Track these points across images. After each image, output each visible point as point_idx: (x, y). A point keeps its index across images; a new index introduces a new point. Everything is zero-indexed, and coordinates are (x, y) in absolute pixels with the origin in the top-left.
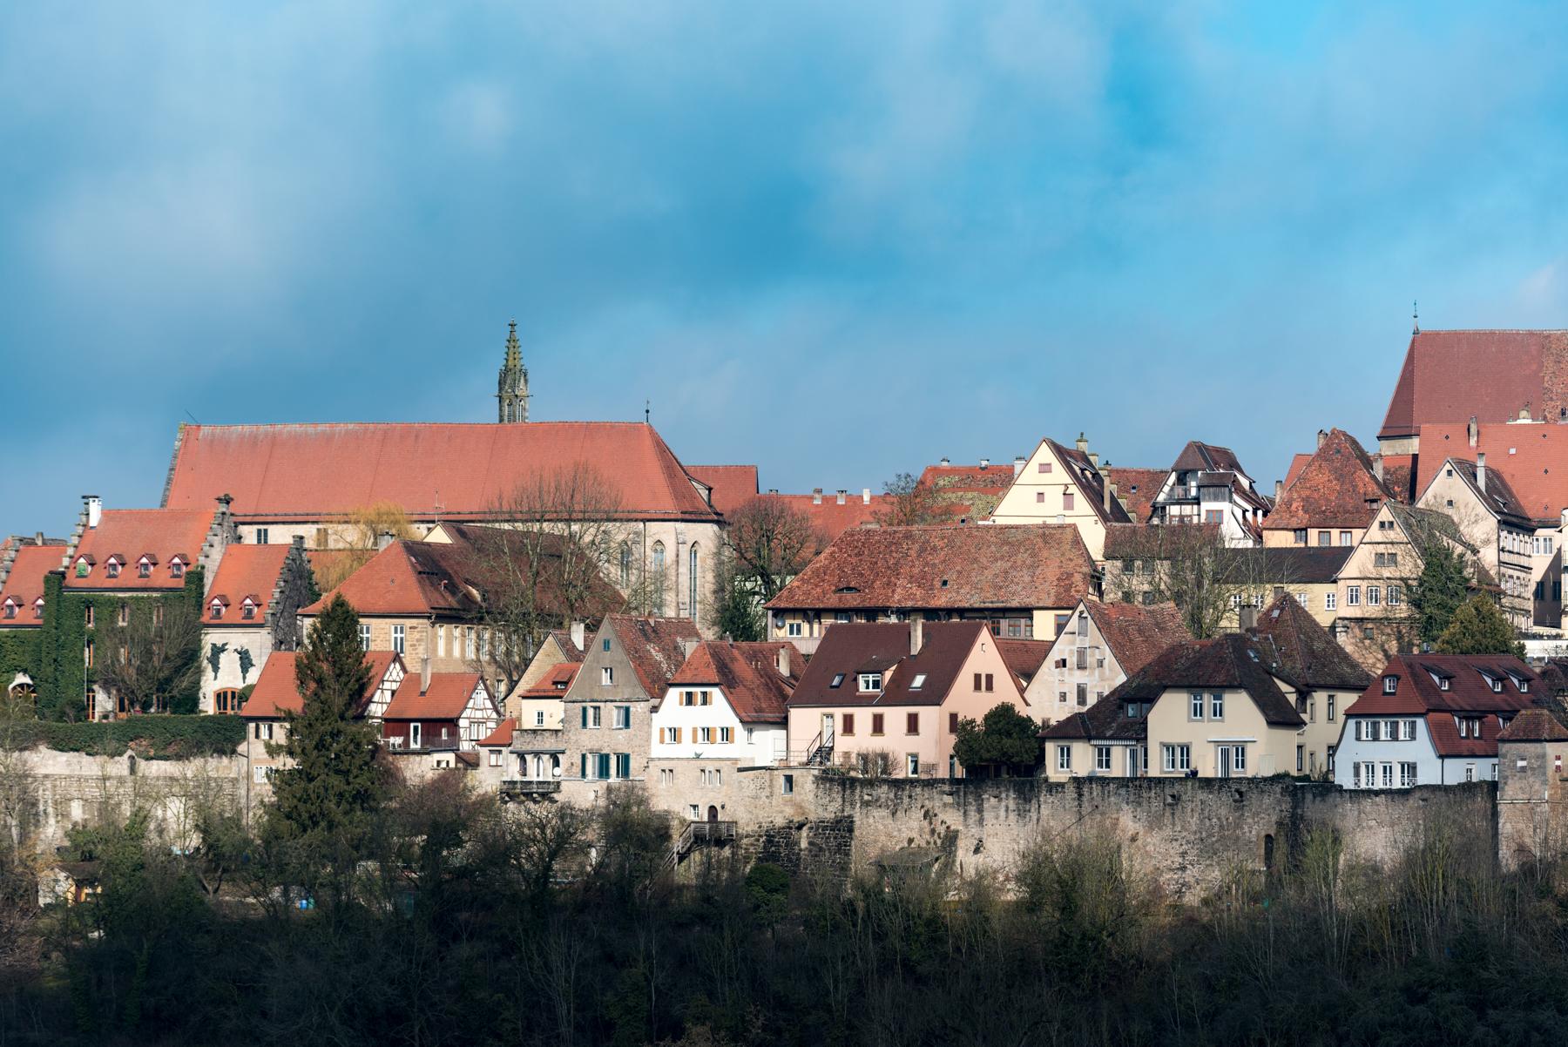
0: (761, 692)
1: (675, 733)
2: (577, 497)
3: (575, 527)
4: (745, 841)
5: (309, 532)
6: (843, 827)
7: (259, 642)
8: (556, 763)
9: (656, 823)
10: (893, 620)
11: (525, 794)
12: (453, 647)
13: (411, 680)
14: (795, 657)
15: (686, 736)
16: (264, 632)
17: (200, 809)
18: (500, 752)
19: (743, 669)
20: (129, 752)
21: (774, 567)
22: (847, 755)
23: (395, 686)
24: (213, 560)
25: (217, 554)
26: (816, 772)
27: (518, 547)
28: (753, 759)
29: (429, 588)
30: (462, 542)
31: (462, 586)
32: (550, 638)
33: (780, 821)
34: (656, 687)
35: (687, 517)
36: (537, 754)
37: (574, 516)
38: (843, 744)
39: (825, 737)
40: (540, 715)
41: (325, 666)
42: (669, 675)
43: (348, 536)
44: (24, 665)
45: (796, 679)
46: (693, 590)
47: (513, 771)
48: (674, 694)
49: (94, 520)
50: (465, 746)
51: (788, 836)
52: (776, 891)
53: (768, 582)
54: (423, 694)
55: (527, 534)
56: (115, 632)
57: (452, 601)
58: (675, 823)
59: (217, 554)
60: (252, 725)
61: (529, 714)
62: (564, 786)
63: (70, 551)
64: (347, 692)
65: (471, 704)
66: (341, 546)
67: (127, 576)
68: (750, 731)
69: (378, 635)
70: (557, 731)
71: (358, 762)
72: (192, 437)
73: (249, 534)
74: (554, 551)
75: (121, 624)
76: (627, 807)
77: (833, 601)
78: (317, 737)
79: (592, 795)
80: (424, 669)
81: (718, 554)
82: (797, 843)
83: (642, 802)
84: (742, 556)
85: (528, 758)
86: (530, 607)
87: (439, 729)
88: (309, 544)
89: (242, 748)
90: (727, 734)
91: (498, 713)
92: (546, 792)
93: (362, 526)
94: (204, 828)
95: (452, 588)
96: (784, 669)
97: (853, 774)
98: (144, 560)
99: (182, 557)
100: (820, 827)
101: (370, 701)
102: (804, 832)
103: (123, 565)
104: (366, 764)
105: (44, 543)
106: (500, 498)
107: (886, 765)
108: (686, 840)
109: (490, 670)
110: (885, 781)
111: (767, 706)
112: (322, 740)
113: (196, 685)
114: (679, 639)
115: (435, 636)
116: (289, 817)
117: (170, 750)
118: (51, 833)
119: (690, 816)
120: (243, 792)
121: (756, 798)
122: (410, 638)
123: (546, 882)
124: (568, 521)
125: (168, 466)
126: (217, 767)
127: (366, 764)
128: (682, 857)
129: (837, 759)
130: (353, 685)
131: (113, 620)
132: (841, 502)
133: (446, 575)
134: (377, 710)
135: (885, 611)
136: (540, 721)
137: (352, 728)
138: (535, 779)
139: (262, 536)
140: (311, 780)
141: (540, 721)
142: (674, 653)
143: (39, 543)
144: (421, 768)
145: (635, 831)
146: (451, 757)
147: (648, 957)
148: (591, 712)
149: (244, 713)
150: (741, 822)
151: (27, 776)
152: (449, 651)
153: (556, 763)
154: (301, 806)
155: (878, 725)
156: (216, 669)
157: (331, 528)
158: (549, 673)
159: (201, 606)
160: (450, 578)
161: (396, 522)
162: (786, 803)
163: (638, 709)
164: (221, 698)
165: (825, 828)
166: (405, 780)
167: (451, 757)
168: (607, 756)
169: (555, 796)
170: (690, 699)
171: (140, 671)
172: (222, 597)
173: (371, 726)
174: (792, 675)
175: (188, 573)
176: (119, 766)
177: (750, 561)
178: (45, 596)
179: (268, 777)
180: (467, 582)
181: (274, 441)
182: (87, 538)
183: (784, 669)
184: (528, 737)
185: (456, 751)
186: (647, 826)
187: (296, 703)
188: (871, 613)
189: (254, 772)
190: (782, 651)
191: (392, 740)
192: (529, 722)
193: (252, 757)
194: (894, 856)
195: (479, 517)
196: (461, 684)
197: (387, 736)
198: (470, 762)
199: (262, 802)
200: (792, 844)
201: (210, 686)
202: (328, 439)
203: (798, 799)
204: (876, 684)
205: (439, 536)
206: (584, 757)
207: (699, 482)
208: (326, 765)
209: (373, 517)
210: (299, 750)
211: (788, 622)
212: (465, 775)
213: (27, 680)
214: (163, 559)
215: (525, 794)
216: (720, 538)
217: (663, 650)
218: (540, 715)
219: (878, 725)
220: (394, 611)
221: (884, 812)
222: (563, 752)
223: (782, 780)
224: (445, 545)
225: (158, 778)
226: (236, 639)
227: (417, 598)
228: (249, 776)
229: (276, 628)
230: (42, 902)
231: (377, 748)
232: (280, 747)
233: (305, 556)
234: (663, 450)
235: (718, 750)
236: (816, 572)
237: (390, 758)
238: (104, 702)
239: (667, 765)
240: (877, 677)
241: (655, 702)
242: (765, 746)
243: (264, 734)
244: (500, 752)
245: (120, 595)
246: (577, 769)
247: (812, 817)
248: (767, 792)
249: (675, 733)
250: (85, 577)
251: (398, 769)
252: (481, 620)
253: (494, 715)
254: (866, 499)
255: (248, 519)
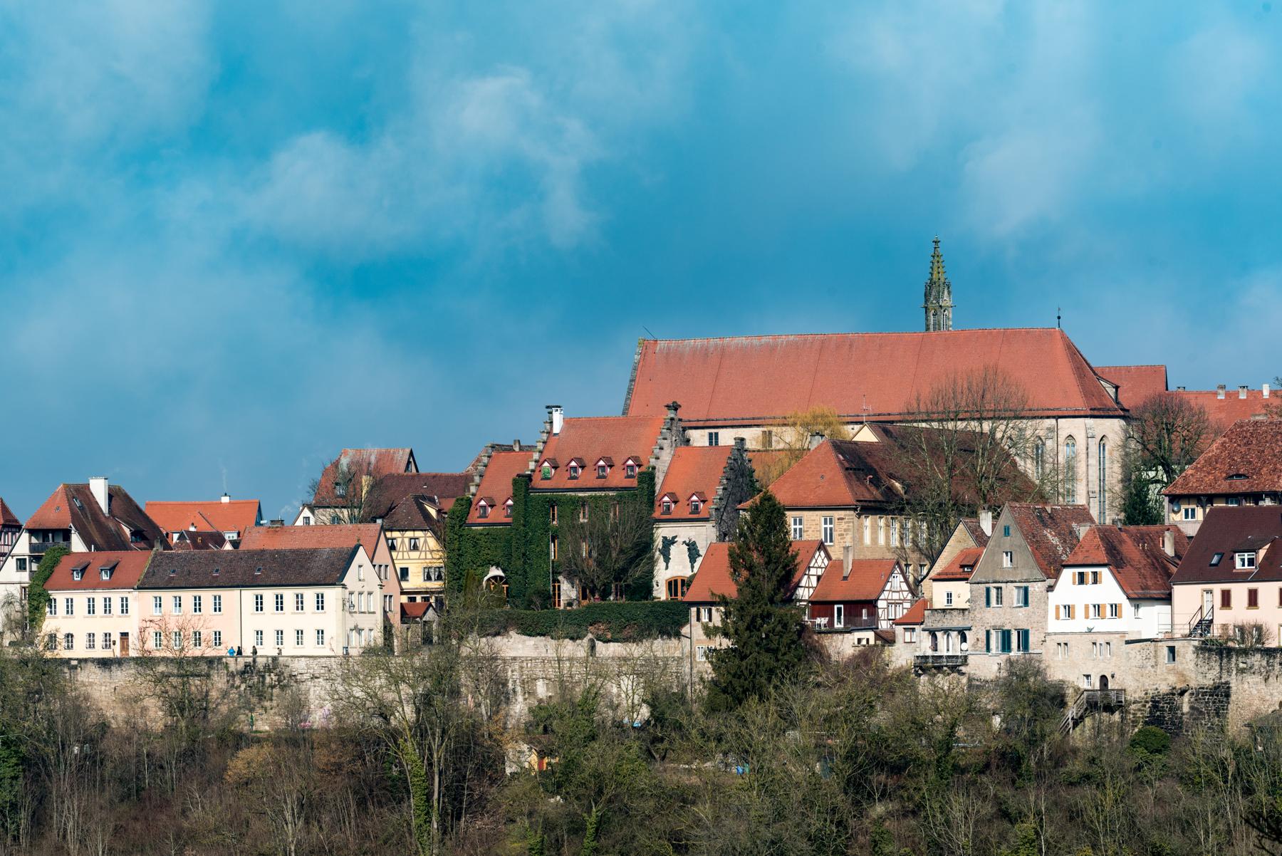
0: (1147, 572)
1: (1069, 610)
2: (988, 396)
3: (987, 426)
4: (1133, 707)
5: (752, 437)
6: (1221, 693)
7: (704, 534)
8: (964, 639)
9: (1052, 692)
10: (1267, 502)
11: (935, 668)
12: (878, 535)
13: (835, 566)
14: (1179, 538)
15: (1080, 612)
16: (709, 525)
17: (648, 685)
18: (913, 630)
19: (1131, 550)
20: (590, 636)
21: (1174, 457)
22: (1225, 627)
23: (820, 572)
24: (663, 461)
25: (666, 456)
26: (1196, 643)
27: (934, 443)
28: (1139, 632)
29: (855, 483)
30: (887, 440)
31: (884, 477)
32: (961, 526)
33: (1164, 689)
34: (1052, 568)
35: (1096, 413)
36: (947, 631)
37: (985, 414)
38: (1222, 618)
39: (1205, 611)
40: (949, 595)
41: (755, 555)
42: (1064, 557)
43: (788, 437)
44: (496, 560)
45: (1180, 558)
46: (1102, 480)
47: (925, 647)
48: (1068, 575)
49: (556, 429)
50: (884, 625)
51: (1171, 702)
52: (1159, 751)
53: (1169, 471)
54: (845, 578)
55: (940, 432)
56: (576, 527)
57: (877, 494)
58: (1070, 691)
59: (666, 456)
60: (694, 610)
61: (938, 593)
62: (971, 660)
63: (536, 456)
64: (774, 578)
65: (888, 587)
66: (781, 446)
67: (587, 478)
68: (1137, 607)
69: (805, 527)
70: (964, 610)
71: (785, 640)
72: (650, 351)
73: (699, 438)
74: (967, 446)
75: (581, 520)
76: (1024, 678)
77: (1223, 487)
78: (748, 619)
79: (996, 667)
80: (846, 556)
81: (1124, 446)
82: (1180, 708)
83: (1038, 672)
84: (1145, 447)
85: (939, 634)
86: (945, 497)
87: (859, 610)
88: (749, 445)
89: (685, 630)
90: (1115, 609)
91: (913, 595)
92: (956, 665)
93: (801, 430)
94: (653, 704)
95: (876, 482)
96: (1169, 550)
97: (1230, 644)
98: (602, 463)
99: (635, 459)
100: (1200, 693)
101: (798, 586)
102: (1186, 697)
103: (583, 467)
104: (793, 642)
105: (521, 448)
106: (918, 400)
107: (1260, 635)
108: (1079, 707)
109: (914, 556)
110: (1258, 650)
111: (1152, 585)
112: (753, 620)
113: (650, 574)
114: (1074, 525)
115: (861, 526)
116: (725, 691)
117: (625, 633)
118: (519, 708)
119: (1084, 685)
120: (687, 670)
121: (1142, 667)
122: (839, 528)
123: (949, 749)
124: (980, 420)
125: (629, 377)
126: (661, 647)
127: (793, 642)
128: (1076, 724)
129: (1216, 631)
130: (780, 572)
131: (574, 515)
132: (1243, 396)
133: (871, 470)
134: (804, 593)
135: (1257, 497)
136: (949, 601)
137: (779, 611)
138: (945, 653)
139: (713, 439)
140: (743, 658)
141: (949, 601)
142: (1070, 538)
143: (517, 449)
144: (845, 646)
145: (1035, 697)
146: (870, 635)
147: (1039, 813)
148: (993, 593)
149: (688, 598)
150: (1129, 690)
151: (496, 659)
152: (875, 539)
153: (964, 639)
154: (736, 682)
155: (1253, 599)
156: (667, 560)
157: (774, 429)
158: (959, 556)
159: (653, 503)
160: (875, 473)
161: (830, 424)
162: (1169, 671)
163: (1036, 589)
164: (672, 585)
165: (1204, 694)
166: (829, 657)
167: (870, 635)
168: (1009, 631)
169: (963, 669)
170: (1082, 579)
171: (599, 563)
172: (671, 495)
173: (798, 608)
174: (1177, 556)
175: (640, 474)
176: (574, 649)
177: (1152, 453)
178: (514, 497)
179: (707, 658)
180: (891, 476)
181: (723, 352)
182: (550, 444)
183: (1169, 550)
184: (939, 616)
185: (875, 629)
186: (1044, 695)
187: (731, 591)
188: (1257, 497)
189: (694, 651)
190: (1167, 534)
191: (818, 621)
192: (939, 602)
193: (694, 639)
194: (1267, 717)
195: (898, 418)
196: (880, 570)
197: (813, 616)
198: (887, 640)
199: (701, 678)
200: (1175, 709)
201: (662, 575)
202: (772, 349)
203: (1180, 667)
204: (1251, 562)
205: (866, 435)
206: (988, 633)
207: (1107, 381)
208: (757, 644)
209: (809, 419)
210: (732, 631)
211: (1183, 507)
212: (882, 651)
213: (500, 573)
214: (618, 462)
215: (935, 668)
216: (1126, 431)
217: (1059, 534)
218: (949, 595)
219: (1253, 599)
220: (823, 503)
221: (1258, 678)
222: (970, 629)
223: (1166, 651)
224: (871, 444)
225: (613, 658)
226: (684, 532)
227: (844, 492)
228: (692, 655)
229: (720, 522)
230: (508, 771)
231: (803, 627)
232: (716, 628)
233: (746, 456)
234: (1073, 353)
235: (1106, 624)
236: (1209, 462)
237: (816, 637)
238: (568, 591)
239: (1062, 639)
240: (1252, 555)
241: (1050, 582)
242: (1152, 620)
243: (705, 619)
244: (913, 630)
245: (581, 494)
246: (982, 644)
247: (1193, 684)
248: (1152, 662)
249: (1069, 610)
250: (550, 479)
251: (823, 647)
252: (901, 511)
253: (910, 596)
254: (1266, 393)
255: (701, 424)
